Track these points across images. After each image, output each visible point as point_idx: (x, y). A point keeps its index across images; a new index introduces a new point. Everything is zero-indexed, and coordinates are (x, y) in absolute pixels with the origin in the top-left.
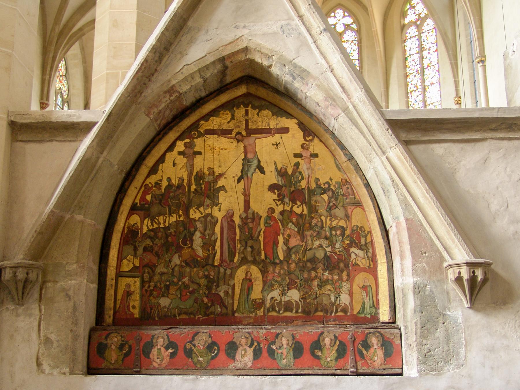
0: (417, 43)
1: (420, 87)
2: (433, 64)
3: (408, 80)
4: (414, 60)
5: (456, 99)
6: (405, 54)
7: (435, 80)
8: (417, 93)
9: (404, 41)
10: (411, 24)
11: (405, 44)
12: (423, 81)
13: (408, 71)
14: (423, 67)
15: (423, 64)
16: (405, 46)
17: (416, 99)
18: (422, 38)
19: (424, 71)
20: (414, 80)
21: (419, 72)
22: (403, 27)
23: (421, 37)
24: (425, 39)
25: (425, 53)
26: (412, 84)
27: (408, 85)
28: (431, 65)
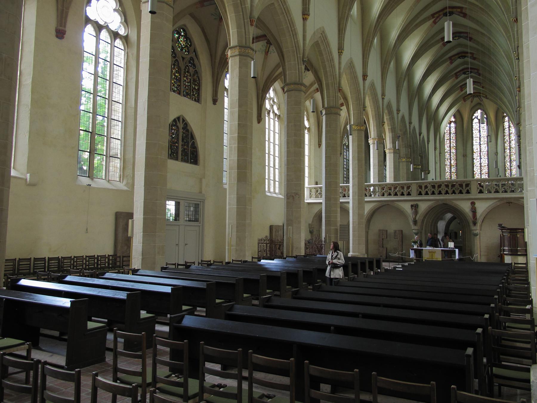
0: (508, 123)
1: (508, 141)
6: (504, 128)
9: (504, 123)
12: (510, 139)
20: (507, 138)
22: (504, 117)
25: (511, 128)
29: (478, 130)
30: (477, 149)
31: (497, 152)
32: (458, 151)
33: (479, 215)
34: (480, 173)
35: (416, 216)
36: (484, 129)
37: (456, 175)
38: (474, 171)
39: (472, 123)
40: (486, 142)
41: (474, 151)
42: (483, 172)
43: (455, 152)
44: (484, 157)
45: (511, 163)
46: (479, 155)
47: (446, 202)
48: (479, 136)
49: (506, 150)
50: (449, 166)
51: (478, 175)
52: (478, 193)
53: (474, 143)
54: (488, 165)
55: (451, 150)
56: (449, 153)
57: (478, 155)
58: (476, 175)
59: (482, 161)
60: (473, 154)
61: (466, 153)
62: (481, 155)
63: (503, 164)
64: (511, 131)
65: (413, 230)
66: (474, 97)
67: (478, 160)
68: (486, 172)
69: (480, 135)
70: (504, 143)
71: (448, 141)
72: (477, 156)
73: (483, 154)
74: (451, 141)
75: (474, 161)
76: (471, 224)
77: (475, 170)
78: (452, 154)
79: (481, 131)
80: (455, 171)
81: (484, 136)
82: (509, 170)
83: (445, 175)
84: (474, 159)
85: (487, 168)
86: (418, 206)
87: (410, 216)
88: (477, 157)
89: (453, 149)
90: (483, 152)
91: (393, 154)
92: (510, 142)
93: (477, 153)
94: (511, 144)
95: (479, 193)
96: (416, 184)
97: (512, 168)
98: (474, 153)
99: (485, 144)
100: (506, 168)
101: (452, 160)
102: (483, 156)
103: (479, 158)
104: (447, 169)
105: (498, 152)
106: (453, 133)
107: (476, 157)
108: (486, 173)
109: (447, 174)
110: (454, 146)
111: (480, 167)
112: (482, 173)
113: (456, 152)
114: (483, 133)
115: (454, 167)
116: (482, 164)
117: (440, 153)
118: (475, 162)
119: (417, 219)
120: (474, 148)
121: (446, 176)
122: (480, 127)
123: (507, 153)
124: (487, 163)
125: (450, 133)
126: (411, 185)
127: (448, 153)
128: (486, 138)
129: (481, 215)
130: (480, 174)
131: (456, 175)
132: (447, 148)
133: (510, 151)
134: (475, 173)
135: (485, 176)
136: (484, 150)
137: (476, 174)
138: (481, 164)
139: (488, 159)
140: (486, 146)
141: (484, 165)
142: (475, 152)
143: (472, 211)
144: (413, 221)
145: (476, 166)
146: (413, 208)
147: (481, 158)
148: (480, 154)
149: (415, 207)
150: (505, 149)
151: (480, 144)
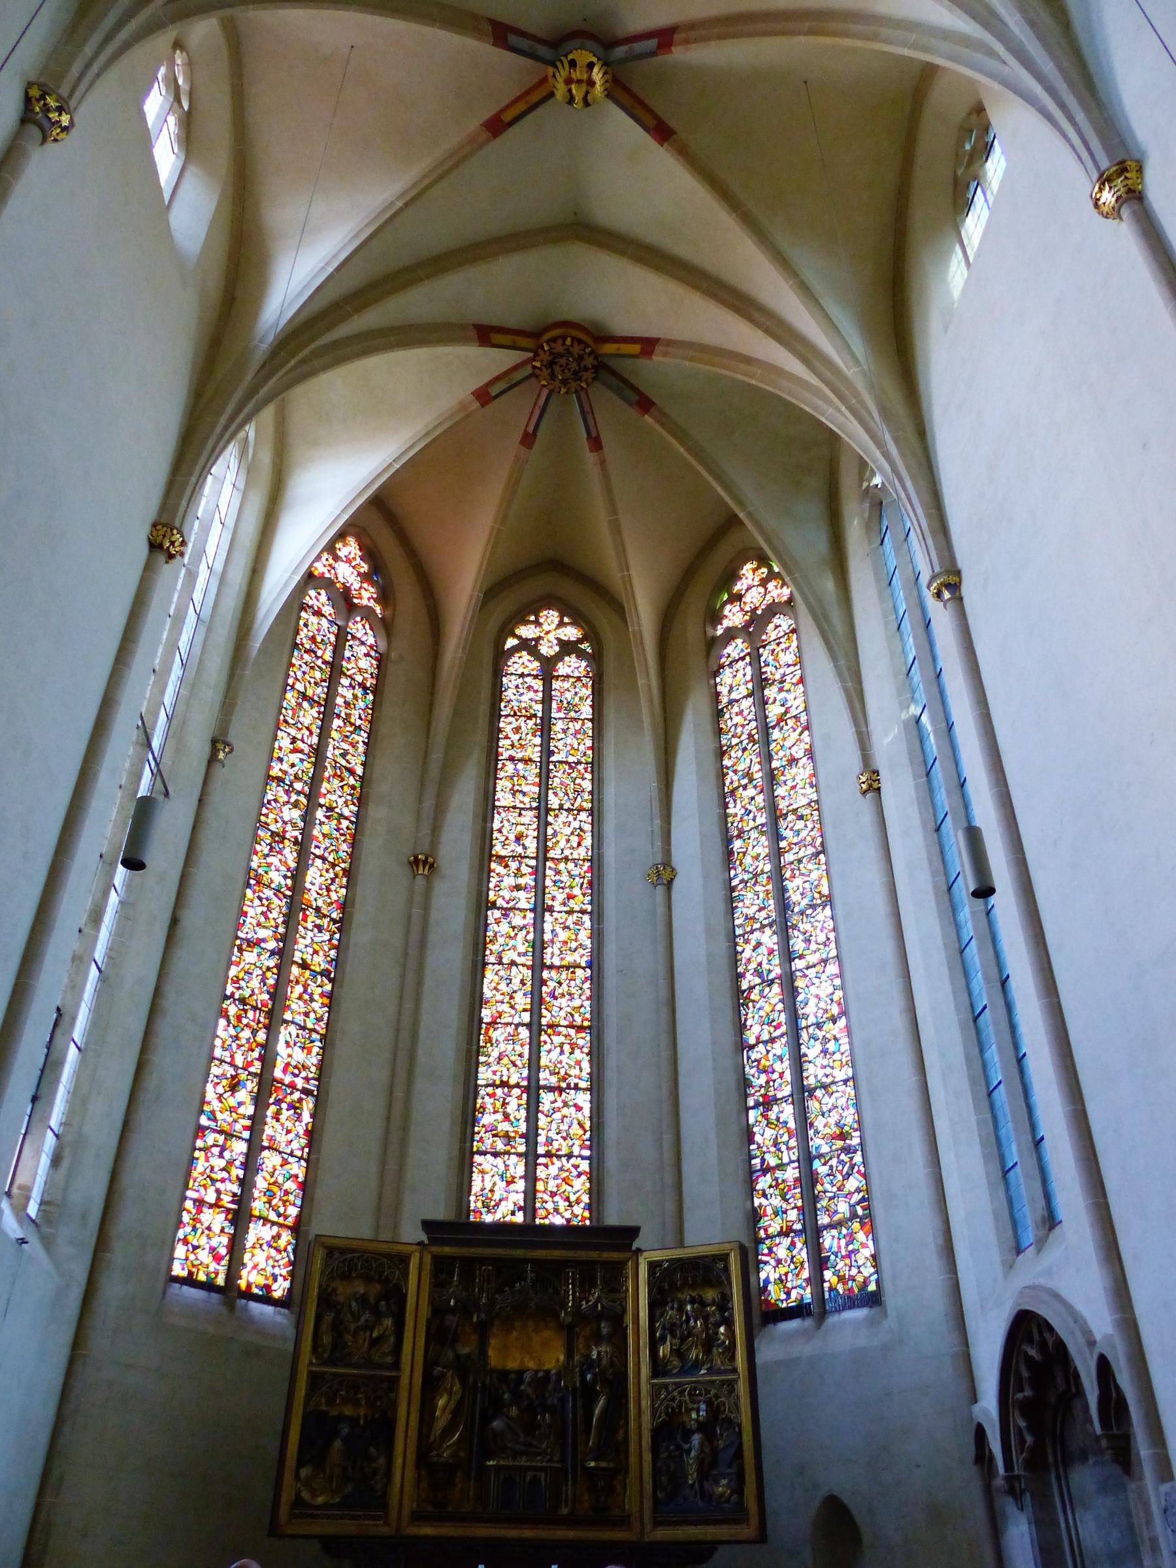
2: (793, 712)
3: (726, 762)
4: (740, 713)
5: (863, 779)
6: (718, 702)
7: (798, 752)
8: (751, 792)
9: (716, 673)
10: (731, 634)
11: (718, 680)
13: (724, 742)
14: (767, 724)
15: (766, 717)
16: (716, 685)
17: (747, 806)
18: (762, 659)
19: (768, 735)
21: (756, 737)
22: (713, 645)
23: (760, 656)
24: (770, 659)
25: (771, 692)
26: (735, 772)
27: (724, 775)
28: (789, 715)
29: (535, 716)
30: (519, 838)
31: (667, 863)
32: (375, 812)
34: (526, 1017)
36: (576, 720)
37: (330, 996)
38: (476, 1000)
39: (498, 673)
40: (586, 796)
41: (498, 849)
42: (557, 1011)
43: (346, 812)
44: (570, 897)
45: (784, 928)
46: (528, 880)
48: (535, 754)
49: (737, 844)
50: (275, 900)
51: (512, 1039)
53: (503, 798)
54: (595, 964)
55: (325, 786)
56: (302, 799)
57: (522, 881)
58: (495, 1035)
59: (548, 927)
60: (483, 873)
61: (434, 843)
62: (548, 882)
63: (723, 945)
64: (774, 711)
67: (517, 920)
68: (578, 1020)
69: (547, 752)
70: (723, 798)
71: (310, 715)
72: (518, 888)
73: (565, 877)
74: (337, 723)
75: (491, 920)
77: (487, 993)
78: (320, 814)
79: (559, 726)
80: (319, 962)
81: (571, 759)
82: (776, 988)
83: (230, 963)
84: (494, 905)
85: (587, 985)
88: (515, 894)
89: (336, 783)
90: (562, 866)
92: (772, 778)
93: (514, 865)
94: (780, 791)
97: (799, 964)
98: (493, 865)
99: (581, 809)
100: (742, 975)
101: (318, 862)
102: (561, 896)
103: (524, 900)
104: (253, 911)
105: (677, 860)
106: (359, 678)
107: (506, 894)
108: (580, 1029)
109: (250, 957)
110: (352, 772)
111: (528, 973)
112: (544, 1021)
113: (357, 815)
114: (570, 740)
115: (320, 928)
116: (549, 951)
117: (214, 742)
118: (493, 927)
120: (496, 825)
121: (233, 971)
122: (547, 700)
123: (748, 860)
124: (588, 943)
125: (335, 670)
127: (294, 797)
128: (588, 776)
130: (529, 1026)
131: (330, 996)
132: (295, 758)
133: (777, 837)
134: (486, 1014)
135: (567, 1048)
136: (567, 852)
137: (493, 1023)
138: (539, 946)
139: (597, 915)
140: (588, 827)
141: (570, 958)
142: (501, 859)
145: (505, 961)
147: (541, 909)
148: (539, 873)
150: (728, 841)
151: (543, 811)
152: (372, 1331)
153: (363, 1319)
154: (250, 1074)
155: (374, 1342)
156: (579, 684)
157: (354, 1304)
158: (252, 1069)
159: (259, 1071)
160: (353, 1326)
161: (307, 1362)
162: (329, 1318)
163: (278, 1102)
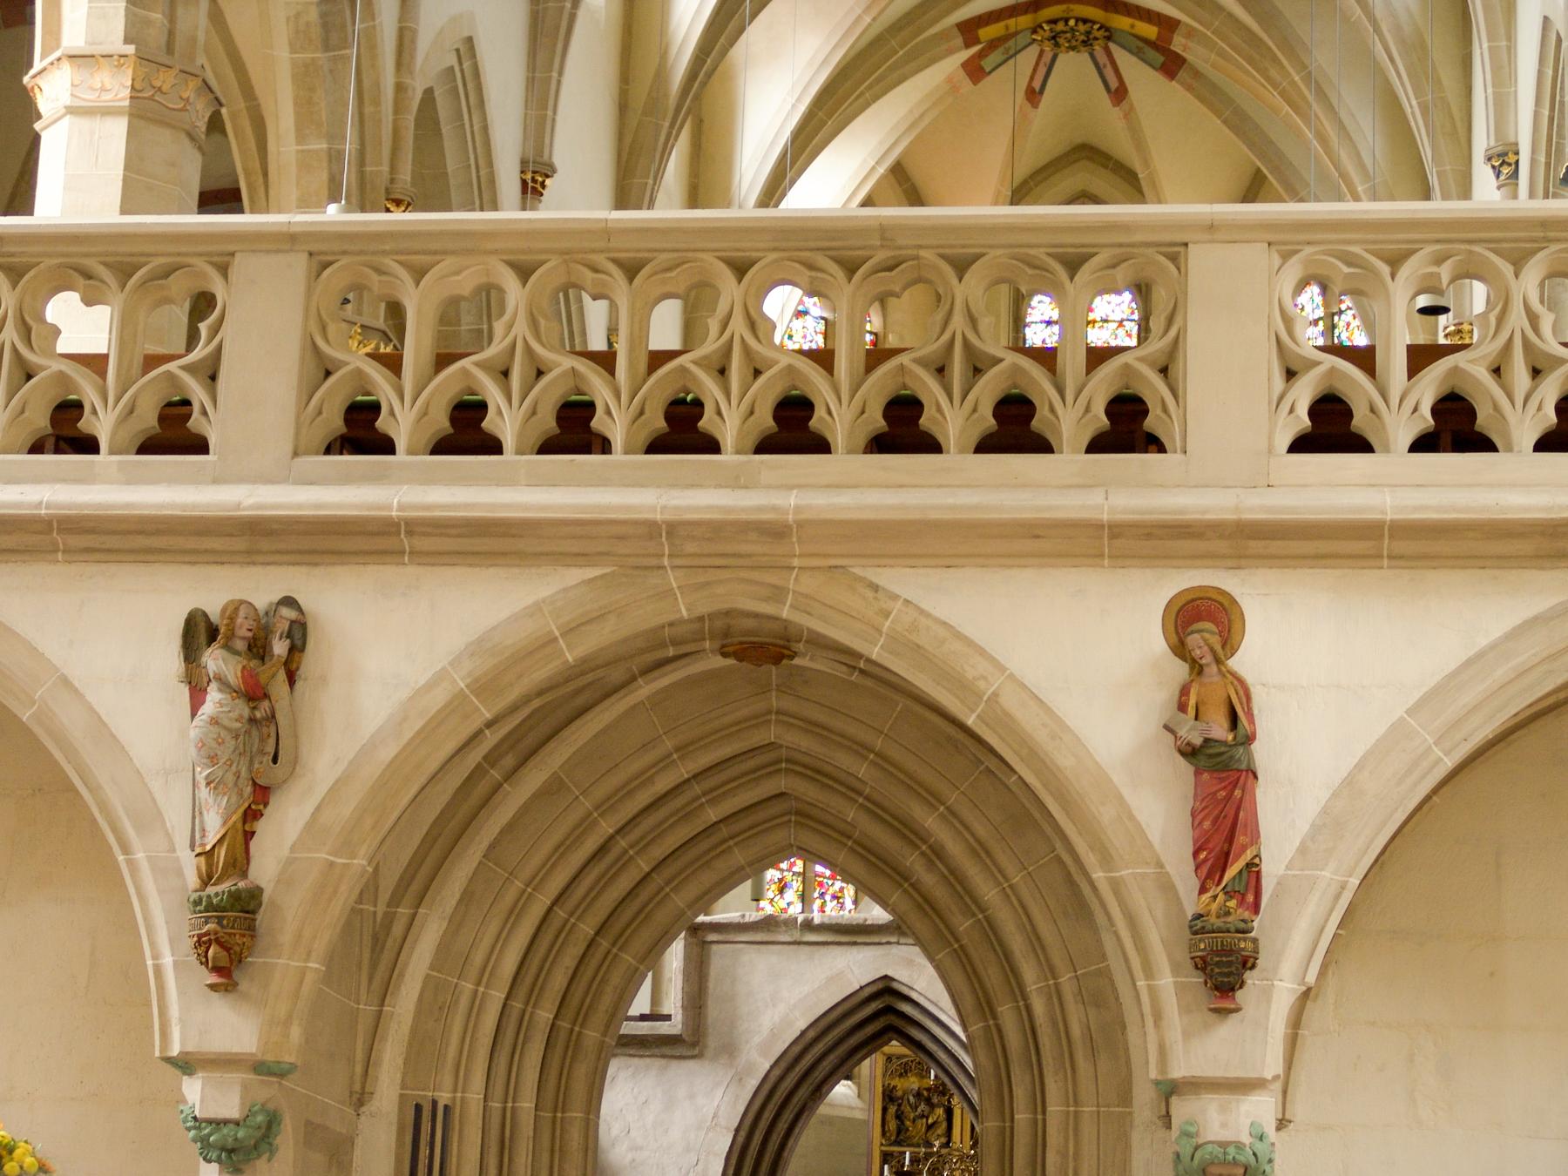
33: (1303, 827)
35: (252, 815)
47: (778, 594)
52: (1286, 440)
65: (186, 1065)
66: (1054, 38)
76: (1166, 981)
86: (298, 635)
87: (151, 818)
91: (118, 129)
95: (1300, 445)
96: (299, 264)
119: (265, 867)
126: (224, 270)
129: (1329, 824)
143: (1190, 753)
144: (206, 907)
146: (214, 660)
149: (258, 648)
152: (927, 1118)
153: (919, 1110)
154: (794, 874)
155: (929, 1127)
156: (1121, 332)
157: (911, 1098)
158: (795, 869)
159: (801, 870)
160: (912, 1116)
161: (879, 1144)
162: (892, 1109)
163: (822, 895)
